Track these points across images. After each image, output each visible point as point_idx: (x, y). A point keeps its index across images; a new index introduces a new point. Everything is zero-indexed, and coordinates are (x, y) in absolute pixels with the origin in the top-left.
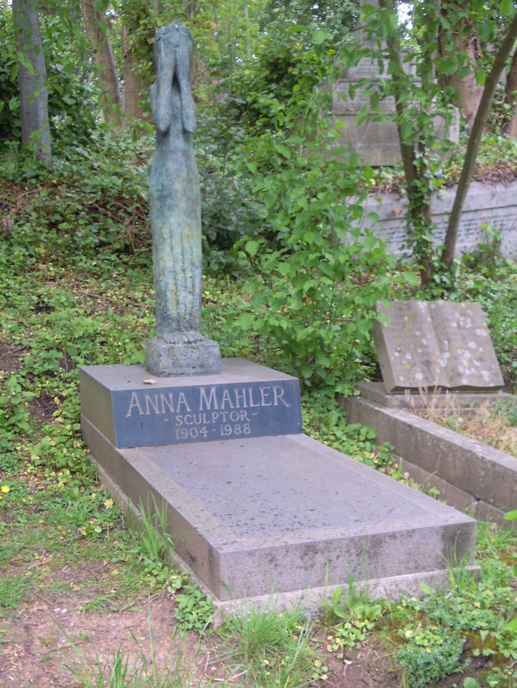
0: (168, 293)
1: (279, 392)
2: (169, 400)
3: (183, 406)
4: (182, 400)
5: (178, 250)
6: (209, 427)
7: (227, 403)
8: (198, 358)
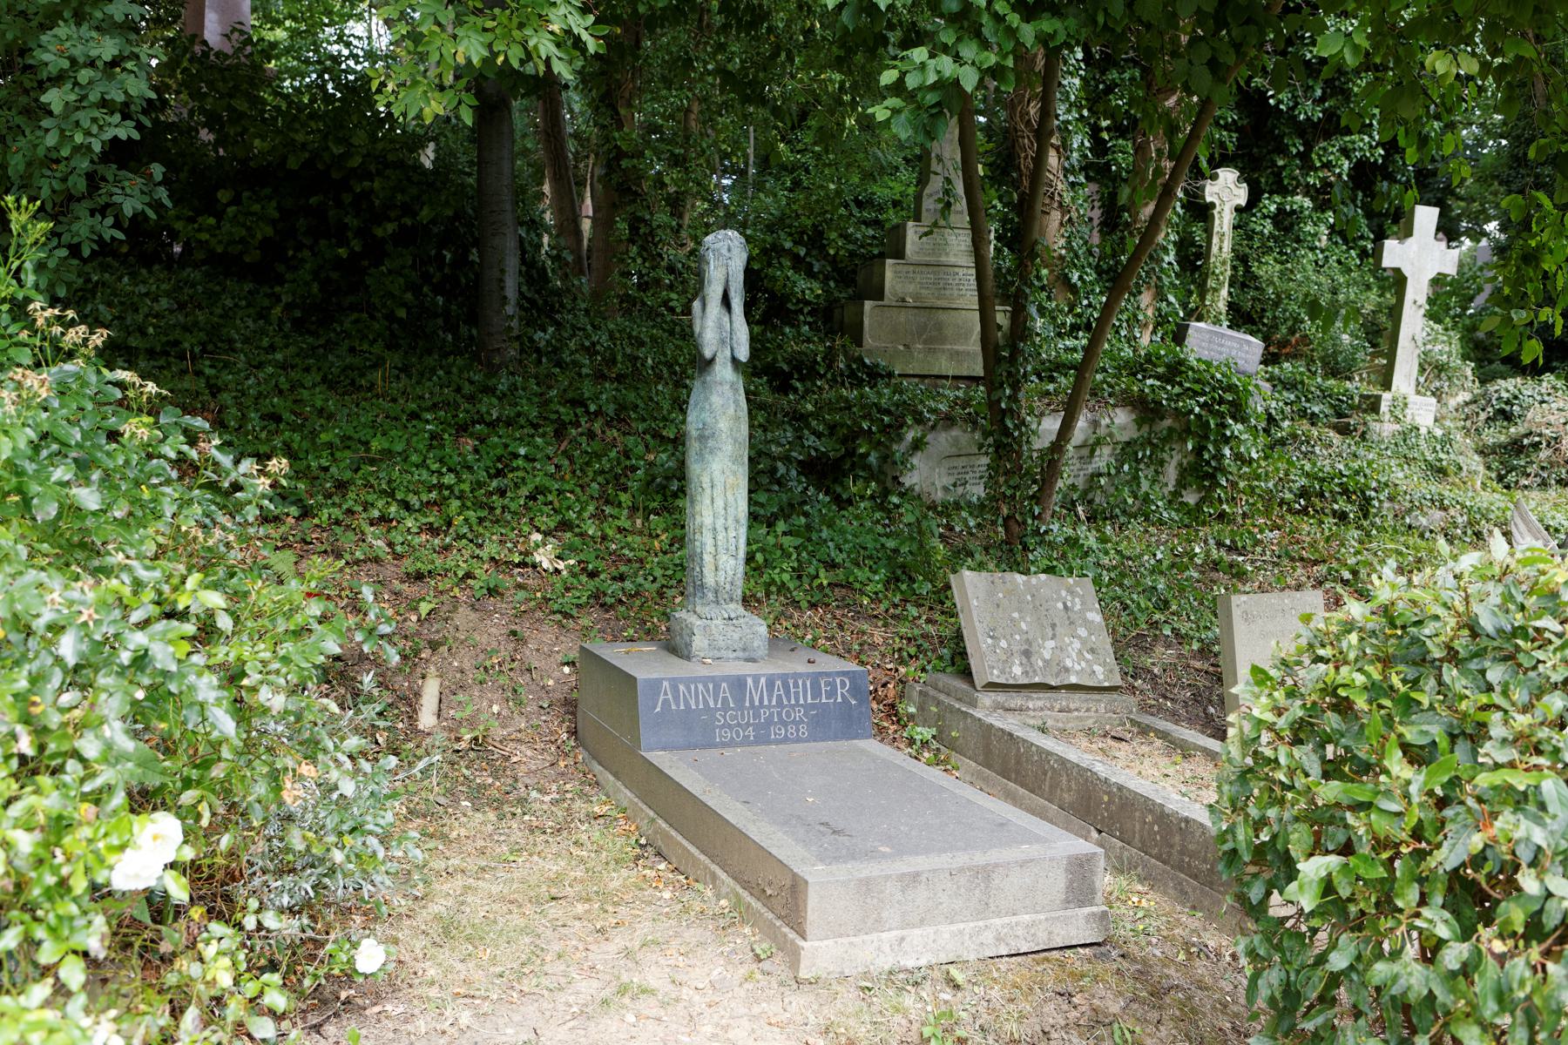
0: (705, 556)
1: (843, 684)
3: (725, 699)
5: (720, 503)
6: (757, 727)
7: (779, 697)
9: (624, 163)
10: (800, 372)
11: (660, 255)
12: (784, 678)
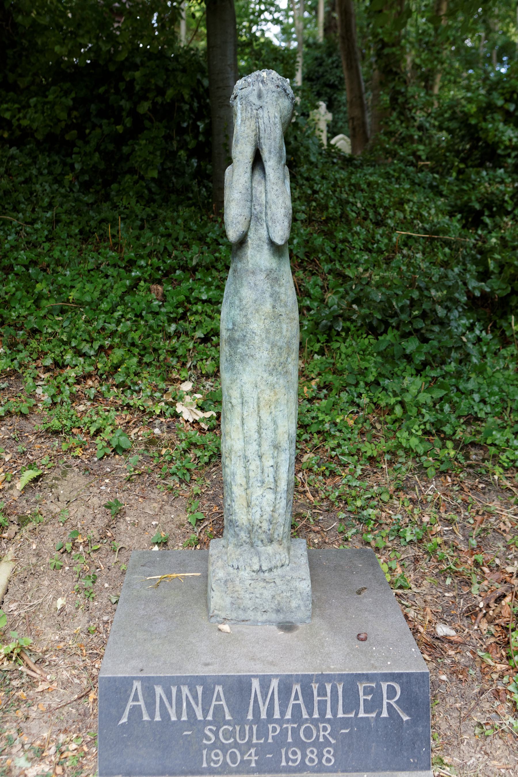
0: (235, 489)
1: (392, 692)
2: (195, 698)
3: (218, 709)
4: (218, 699)
5: (252, 424)
6: (261, 750)
7: (296, 707)
8: (273, 597)
9: (386, 51)
10: (490, 209)
11: (413, 118)
12: (306, 681)
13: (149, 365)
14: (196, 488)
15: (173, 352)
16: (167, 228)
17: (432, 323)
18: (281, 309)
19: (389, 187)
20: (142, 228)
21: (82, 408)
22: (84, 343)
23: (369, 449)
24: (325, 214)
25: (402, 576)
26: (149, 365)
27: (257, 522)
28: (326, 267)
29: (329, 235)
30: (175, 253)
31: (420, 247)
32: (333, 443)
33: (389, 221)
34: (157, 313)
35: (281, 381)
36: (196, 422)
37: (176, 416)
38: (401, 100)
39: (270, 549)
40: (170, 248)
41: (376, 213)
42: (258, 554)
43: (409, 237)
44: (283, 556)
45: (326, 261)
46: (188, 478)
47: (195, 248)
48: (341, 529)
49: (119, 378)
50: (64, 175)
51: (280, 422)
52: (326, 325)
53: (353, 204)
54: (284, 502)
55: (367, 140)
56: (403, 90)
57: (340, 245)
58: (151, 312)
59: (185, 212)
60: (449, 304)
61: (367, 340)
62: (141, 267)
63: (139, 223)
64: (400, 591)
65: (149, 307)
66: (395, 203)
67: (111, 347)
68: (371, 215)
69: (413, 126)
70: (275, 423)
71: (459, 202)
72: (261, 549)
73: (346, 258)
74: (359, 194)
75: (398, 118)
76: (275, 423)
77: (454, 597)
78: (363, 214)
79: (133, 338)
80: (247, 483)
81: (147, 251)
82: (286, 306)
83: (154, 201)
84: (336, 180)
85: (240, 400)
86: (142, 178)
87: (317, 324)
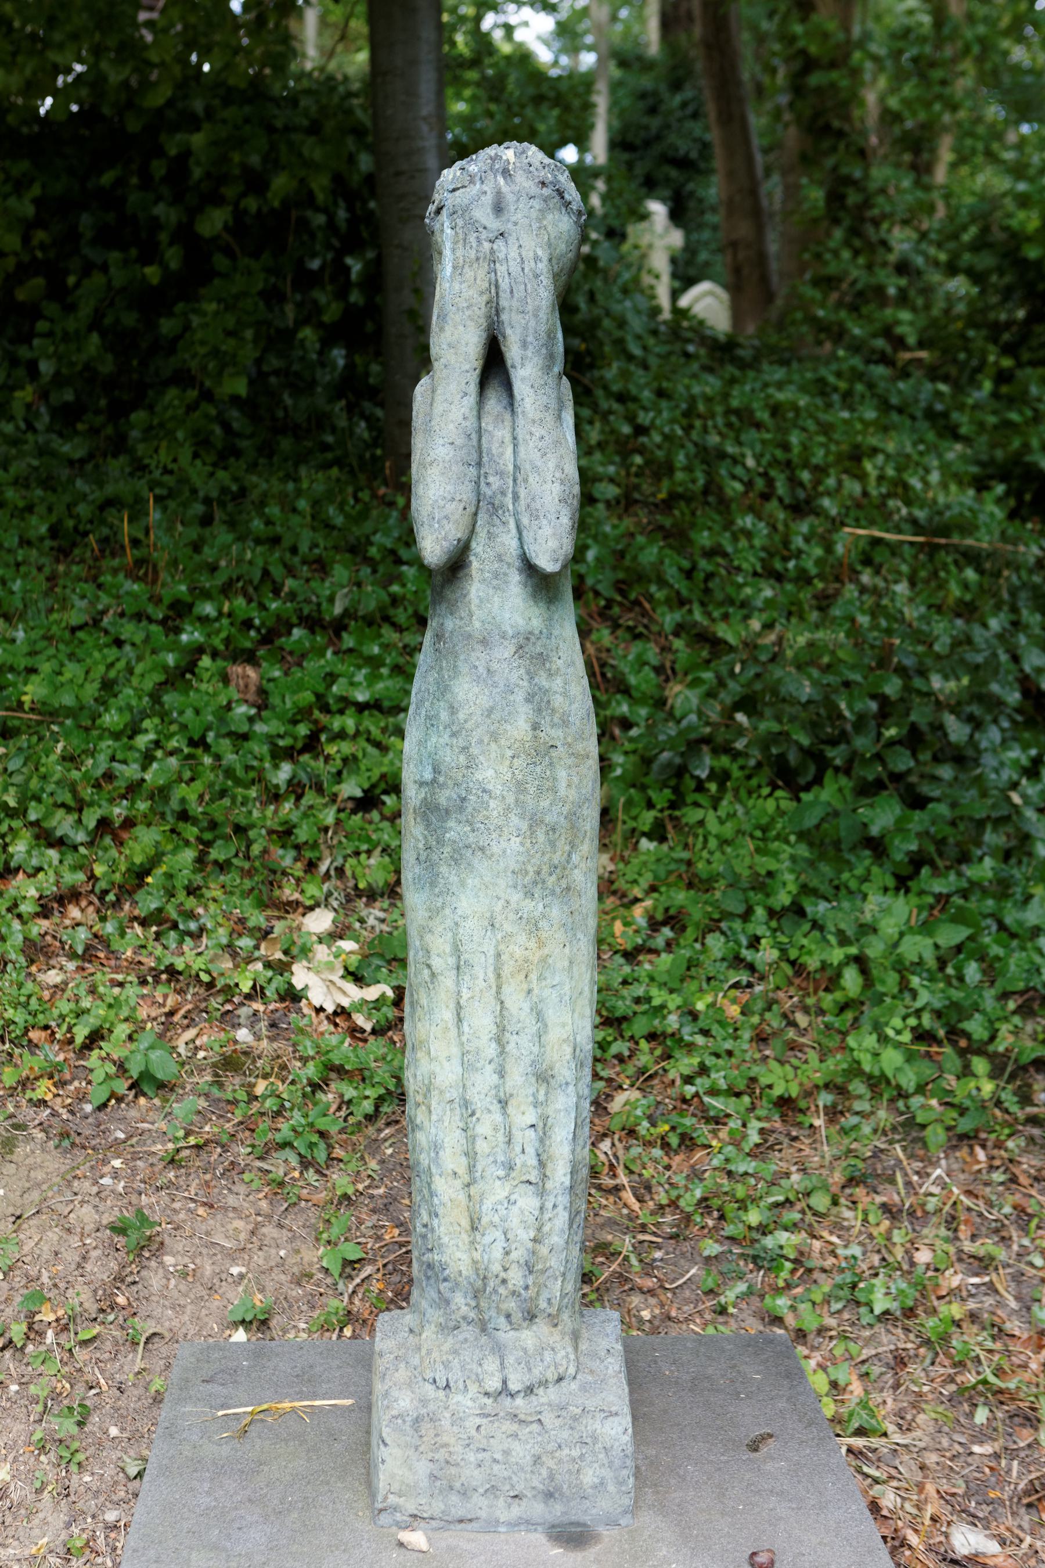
0: (440, 1184)
5: (481, 1021)
8: (537, 1460)
9: (815, 79)
11: (884, 243)
13: (223, 867)
14: (341, 1181)
15: (285, 834)
16: (269, 522)
17: (936, 759)
18: (553, 732)
19: (826, 417)
20: (206, 521)
21: (53, 977)
22: (60, 813)
23: (780, 1080)
24: (665, 484)
25: (863, 1404)
26: (223, 867)
27: (496, 1268)
28: (669, 619)
29: (677, 537)
30: (290, 584)
31: (904, 568)
32: (687, 1064)
33: (826, 502)
34: (245, 737)
35: (555, 912)
36: (342, 1012)
37: (292, 996)
38: (853, 198)
39: (528, 1337)
40: (277, 572)
41: (794, 482)
42: (499, 1350)
43: (876, 542)
44: (563, 1355)
45: (668, 602)
46: (321, 1155)
47: (340, 573)
48: (710, 1283)
49: (149, 902)
50: (13, 389)
51: (551, 1015)
52: (669, 764)
53: (736, 461)
54: (562, 1218)
55: (769, 297)
56: (857, 174)
57: (703, 564)
58: (230, 734)
59: (314, 481)
60: (975, 709)
61: (773, 803)
62: (204, 620)
63: (199, 508)
64: (859, 1442)
65: (222, 720)
66: (840, 458)
67: (129, 823)
68: (781, 488)
69: (885, 264)
70: (539, 1016)
71: (999, 454)
72: (506, 1336)
73: (719, 596)
74: (751, 435)
75: (847, 243)
76: (539, 1016)
77: (997, 1456)
78: (760, 483)
79: (183, 800)
80: (471, 1169)
81: (220, 579)
82: (565, 723)
83: (237, 453)
84: (692, 400)
85: (452, 961)
86: (207, 396)
87: (647, 762)
